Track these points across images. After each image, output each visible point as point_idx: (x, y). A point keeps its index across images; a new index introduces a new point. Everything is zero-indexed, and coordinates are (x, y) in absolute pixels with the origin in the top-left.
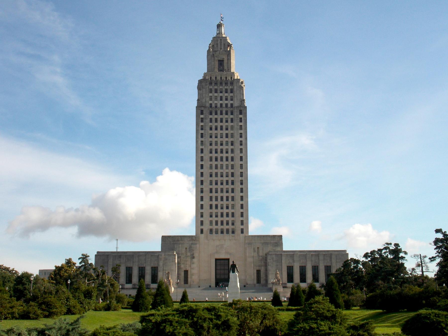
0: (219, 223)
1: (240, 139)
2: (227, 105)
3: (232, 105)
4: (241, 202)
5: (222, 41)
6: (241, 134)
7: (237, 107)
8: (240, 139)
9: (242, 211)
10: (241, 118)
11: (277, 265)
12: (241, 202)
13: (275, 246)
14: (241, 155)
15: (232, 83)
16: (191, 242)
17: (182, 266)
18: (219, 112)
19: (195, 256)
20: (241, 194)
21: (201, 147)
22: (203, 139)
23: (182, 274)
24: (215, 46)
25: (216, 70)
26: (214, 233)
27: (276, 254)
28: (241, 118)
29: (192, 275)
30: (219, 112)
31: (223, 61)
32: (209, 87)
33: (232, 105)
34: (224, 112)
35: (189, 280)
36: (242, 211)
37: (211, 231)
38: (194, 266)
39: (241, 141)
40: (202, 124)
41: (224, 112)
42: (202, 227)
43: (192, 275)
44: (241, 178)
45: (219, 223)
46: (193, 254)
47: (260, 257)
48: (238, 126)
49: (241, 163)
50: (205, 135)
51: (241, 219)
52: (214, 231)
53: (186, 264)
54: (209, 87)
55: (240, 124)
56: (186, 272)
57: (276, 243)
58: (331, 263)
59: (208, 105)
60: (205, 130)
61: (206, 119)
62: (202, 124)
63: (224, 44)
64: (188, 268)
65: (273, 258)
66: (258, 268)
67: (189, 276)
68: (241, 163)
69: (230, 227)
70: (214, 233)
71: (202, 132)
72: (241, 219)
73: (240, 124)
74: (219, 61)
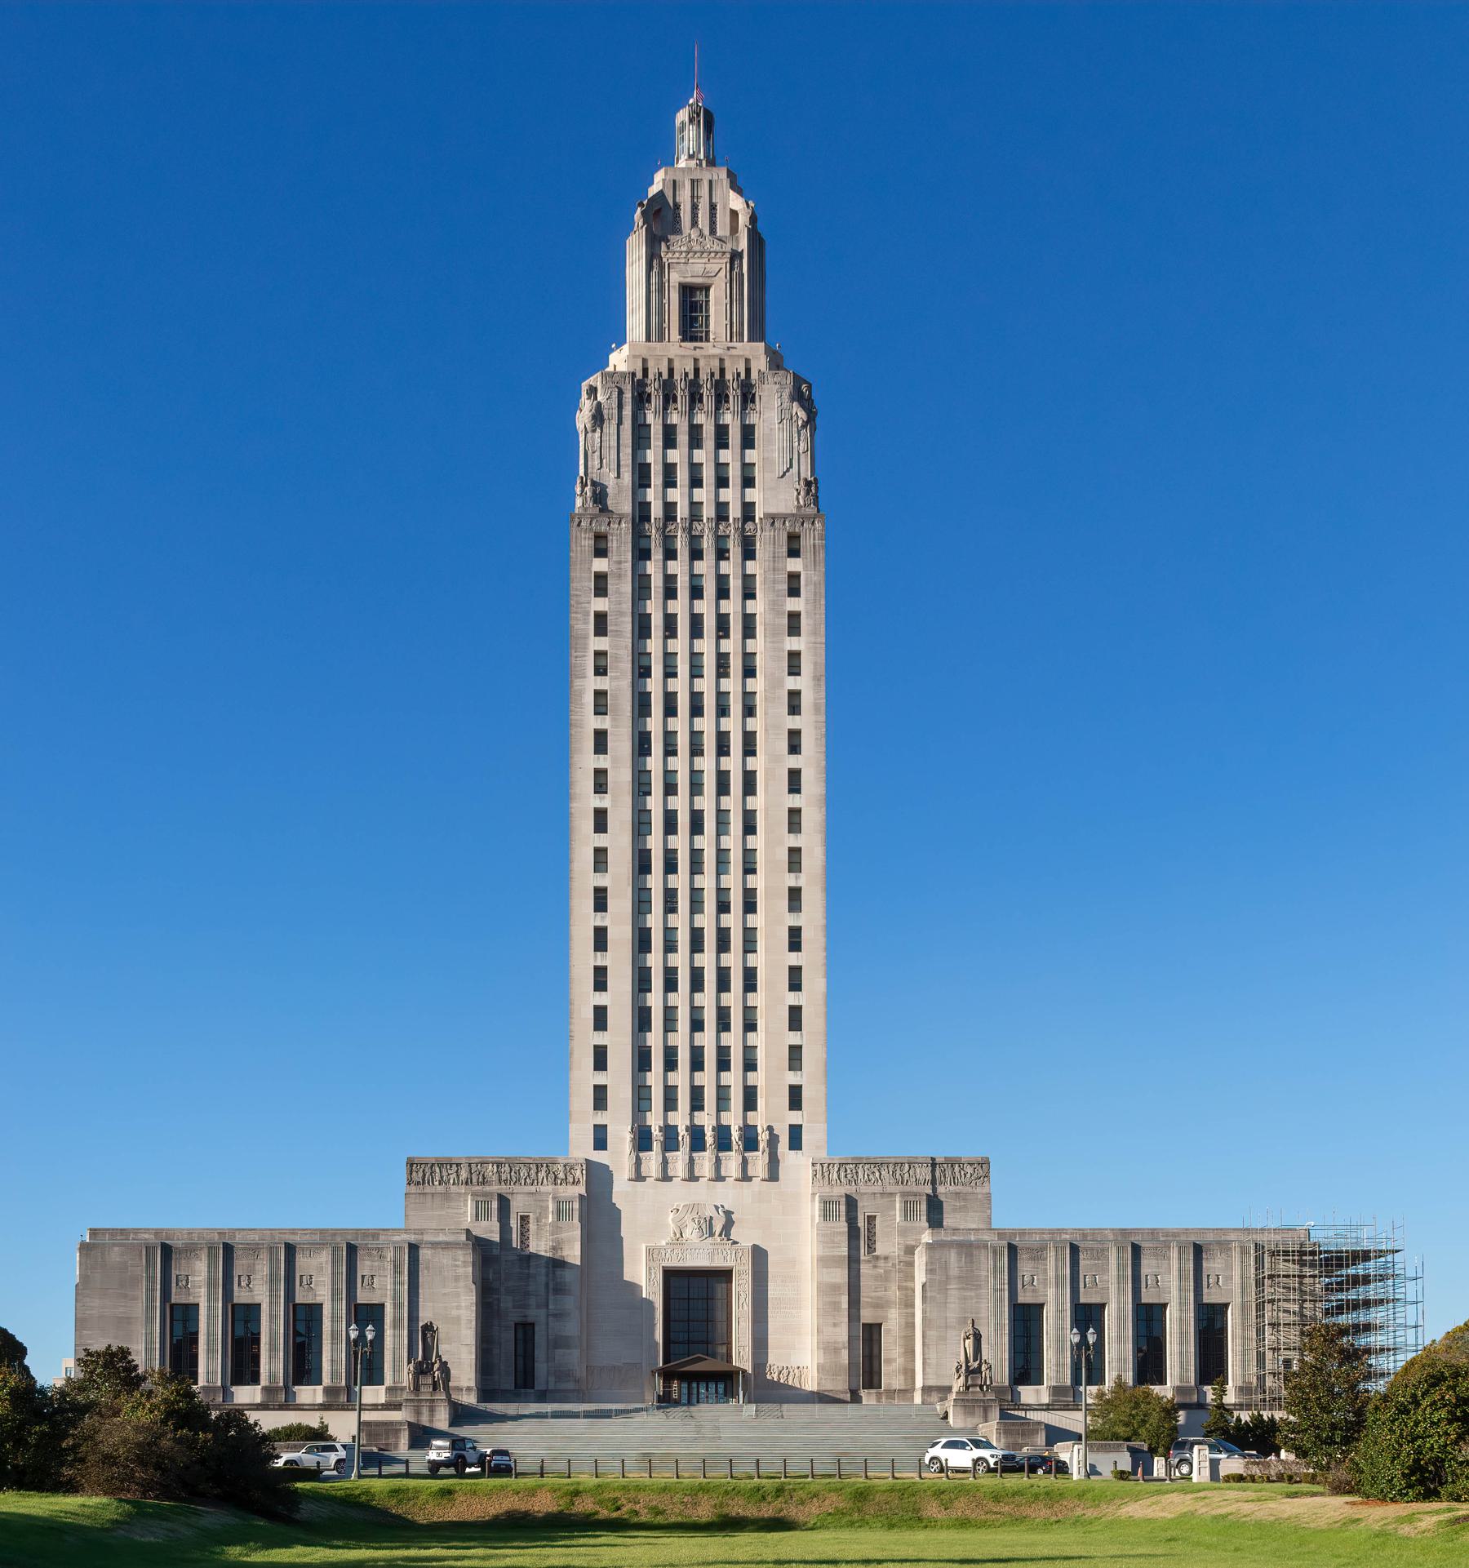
1: (792, 683)
3: (748, 509)
4: (793, 999)
5: (704, 191)
7: (773, 518)
8: (792, 683)
9: (794, 1038)
10: (794, 577)
11: (965, 1298)
12: (793, 999)
14: (794, 762)
15: (748, 397)
17: (507, 1302)
20: (794, 959)
21: (594, 723)
23: (507, 1338)
25: (675, 334)
28: (794, 577)
29: (559, 1342)
35: (541, 1368)
36: (794, 1038)
38: (569, 1303)
39: (794, 695)
40: (601, 604)
43: (559, 1342)
44: (791, 880)
48: (779, 613)
51: (793, 1078)
53: (527, 1294)
55: (793, 604)
56: (525, 1330)
62: (601, 604)
64: (535, 1314)
65: (945, 1267)
67: (540, 1354)
68: (795, 801)
70: (656, 1146)
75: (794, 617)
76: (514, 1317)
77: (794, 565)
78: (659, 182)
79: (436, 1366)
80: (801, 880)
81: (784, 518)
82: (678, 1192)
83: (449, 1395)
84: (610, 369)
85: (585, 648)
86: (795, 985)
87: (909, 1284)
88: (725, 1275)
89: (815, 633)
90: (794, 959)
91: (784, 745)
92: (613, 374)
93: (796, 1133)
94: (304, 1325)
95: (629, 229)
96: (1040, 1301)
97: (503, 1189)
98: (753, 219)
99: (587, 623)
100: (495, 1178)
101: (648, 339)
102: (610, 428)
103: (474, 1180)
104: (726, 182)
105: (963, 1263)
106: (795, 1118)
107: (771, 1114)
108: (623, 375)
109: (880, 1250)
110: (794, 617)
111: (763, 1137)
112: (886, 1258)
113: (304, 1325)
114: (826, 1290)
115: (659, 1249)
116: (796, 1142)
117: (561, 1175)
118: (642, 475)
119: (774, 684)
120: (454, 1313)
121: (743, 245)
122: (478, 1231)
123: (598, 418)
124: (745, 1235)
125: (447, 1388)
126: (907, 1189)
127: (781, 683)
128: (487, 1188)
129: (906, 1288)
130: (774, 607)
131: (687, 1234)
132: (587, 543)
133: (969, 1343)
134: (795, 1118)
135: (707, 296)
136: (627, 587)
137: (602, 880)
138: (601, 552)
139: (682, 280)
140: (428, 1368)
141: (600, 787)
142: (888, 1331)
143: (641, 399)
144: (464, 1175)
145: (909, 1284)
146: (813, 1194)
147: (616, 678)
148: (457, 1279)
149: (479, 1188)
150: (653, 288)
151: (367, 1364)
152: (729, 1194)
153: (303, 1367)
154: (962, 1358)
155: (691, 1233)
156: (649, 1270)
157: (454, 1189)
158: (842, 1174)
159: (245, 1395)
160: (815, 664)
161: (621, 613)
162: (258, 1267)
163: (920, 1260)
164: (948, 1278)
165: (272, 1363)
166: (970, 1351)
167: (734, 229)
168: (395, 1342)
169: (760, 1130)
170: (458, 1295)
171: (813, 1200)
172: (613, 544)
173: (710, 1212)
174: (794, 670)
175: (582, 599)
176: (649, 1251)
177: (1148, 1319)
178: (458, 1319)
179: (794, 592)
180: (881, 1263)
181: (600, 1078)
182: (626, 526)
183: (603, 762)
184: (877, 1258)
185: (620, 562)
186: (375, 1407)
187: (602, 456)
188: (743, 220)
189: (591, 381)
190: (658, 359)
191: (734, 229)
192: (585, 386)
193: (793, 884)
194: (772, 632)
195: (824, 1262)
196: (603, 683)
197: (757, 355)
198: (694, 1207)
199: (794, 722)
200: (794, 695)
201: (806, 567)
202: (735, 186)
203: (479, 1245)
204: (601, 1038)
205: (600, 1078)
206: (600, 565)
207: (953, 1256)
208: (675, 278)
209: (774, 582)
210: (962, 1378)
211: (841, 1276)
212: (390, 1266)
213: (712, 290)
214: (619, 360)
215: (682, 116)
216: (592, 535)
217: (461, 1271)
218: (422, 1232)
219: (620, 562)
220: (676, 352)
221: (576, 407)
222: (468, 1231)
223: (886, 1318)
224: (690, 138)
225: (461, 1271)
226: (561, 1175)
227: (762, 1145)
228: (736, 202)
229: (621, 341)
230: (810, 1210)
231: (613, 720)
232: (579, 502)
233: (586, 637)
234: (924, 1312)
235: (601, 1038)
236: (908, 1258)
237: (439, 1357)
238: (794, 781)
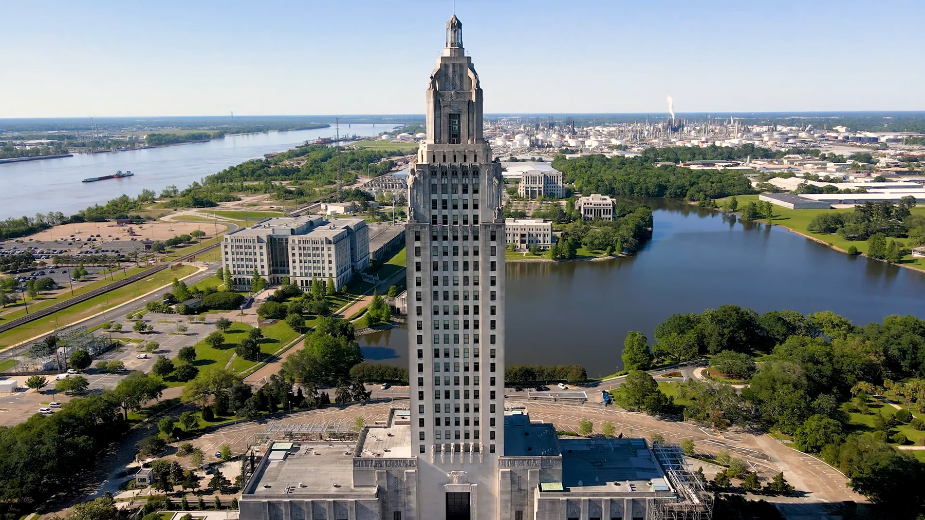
7: (486, 226)
9: (492, 416)
17: (390, 505)
21: (417, 304)
32: (430, 181)
40: (418, 259)
54: (430, 181)
55: (492, 259)
60: (425, 271)
61: (425, 248)
62: (418, 259)
66: (518, 509)
75: (493, 264)
76: (394, 509)
77: (493, 243)
80: (495, 361)
110: (493, 264)
116: (493, 451)
119: (485, 289)
127: (488, 289)
130: (485, 259)
132: (413, 236)
138: (418, 239)
172: (422, 236)
174: (493, 283)
179: (493, 254)
181: (422, 430)
183: (420, 318)
196: (419, 289)
205: (422, 430)
238: (493, 339)
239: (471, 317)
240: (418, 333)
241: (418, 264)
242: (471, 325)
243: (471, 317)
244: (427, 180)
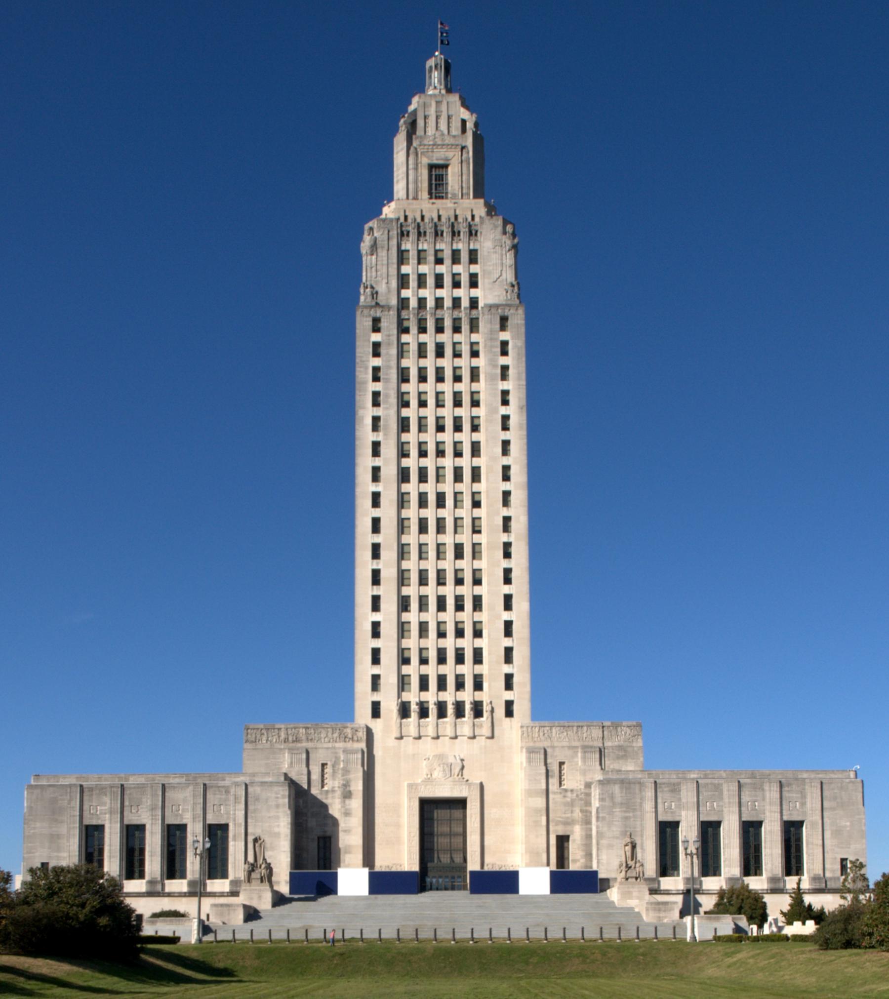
0: (433, 684)
1: (503, 410)
2: (456, 302)
3: (474, 303)
5: (444, 107)
6: (505, 393)
7: (490, 307)
8: (503, 410)
9: (508, 642)
11: (627, 818)
12: (506, 616)
13: (619, 758)
14: (505, 461)
15: (472, 233)
16: (340, 745)
18: (430, 325)
19: (352, 788)
20: (507, 590)
21: (372, 437)
22: (378, 412)
24: (420, 123)
25: (425, 195)
26: (414, 715)
27: (622, 782)
30: (430, 325)
31: (446, 166)
33: (474, 303)
34: (448, 324)
37: (404, 711)
39: (505, 418)
40: (377, 362)
41: (448, 324)
42: (376, 697)
45: (433, 684)
46: (346, 785)
47: (569, 794)
48: (495, 366)
49: (506, 486)
50: (387, 396)
51: (507, 669)
52: (414, 707)
54: (399, 246)
55: (504, 361)
57: (620, 748)
58: (804, 813)
59: (394, 302)
60: (387, 381)
62: (377, 362)
63: (449, 117)
65: (612, 797)
68: (506, 486)
69: (467, 696)
71: (378, 387)
72: (507, 669)
73: (504, 361)
74: (431, 167)
78: (415, 103)
79: (263, 866)
80: (512, 538)
81: (497, 306)
82: (427, 746)
83: (271, 886)
84: (383, 216)
85: (366, 390)
86: (508, 606)
87: (588, 808)
88: (460, 803)
89: (519, 379)
90: (507, 590)
91: (499, 450)
92: (384, 220)
93: (509, 705)
94: (174, 835)
95: (395, 131)
96: (677, 819)
97: (309, 745)
98: (476, 125)
99: (366, 373)
100: (304, 737)
101: (408, 198)
102: (383, 253)
103: (290, 739)
104: (458, 103)
105: (624, 794)
106: (508, 695)
107: (493, 694)
108: (391, 220)
109: (567, 785)
110: (505, 369)
111: (486, 708)
112: (572, 791)
113: (174, 835)
114: (531, 812)
115: (417, 785)
116: (509, 713)
117: (350, 736)
118: (403, 282)
119: (492, 411)
120: (276, 830)
121: (469, 141)
122: (293, 776)
123: (374, 247)
124: (475, 776)
125: (270, 881)
126: (586, 743)
127: (496, 411)
128: (299, 745)
129: (586, 811)
130: (492, 363)
131: (436, 774)
132: (369, 323)
133: (628, 848)
134: (508, 695)
135: (447, 171)
136: (394, 351)
137: (377, 539)
138: (376, 329)
139: (430, 162)
140: (258, 869)
141: (376, 478)
142: (574, 841)
143: (403, 234)
144: (283, 736)
145: (588, 808)
146: (522, 748)
147: (387, 409)
148: (278, 806)
149: (294, 745)
150: (411, 166)
151: (215, 863)
152: (462, 749)
153: (173, 866)
154: (624, 859)
155: (437, 774)
156: (410, 799)
157: (278, 746)
158: (541, 734)
159: (132, 886)
160: (519, 398)
161: (389, 367)
162: (144, 800)
163: (595, 793)
164: (614, 803)
165: (153, 864)
166: (629, 854)
167: (464, 130)
168: (236, 850)
169: (485, 704)
170: (278, 817)
171: (522, 752)
172: (383, 324)
173: (451, 760)
175: (364, 359)
176: (410, 786)
177: (751, 831)
178: (277, 835)
179: (504, 353)
180: (569, 794)
181: (376, 670)
182: (393, 313)
184: (566, 790)
185: (389, 336)
186: (222, 895)
187: (377, 271)
188: (470, 125)
189: (370, 224)
190: (414, 211)
191: (464, 130)
192: (367, 227)
193: (506, 540)
194: (491, 378)
195: (530, 793)
197: (479, 208)
198: (440, 757)
199: (505, 435)
200: (505, 418)
201: (513, 338)
202: (464, 105)
203: (293, 785)
204: (376, 643)
205: (376, 670)
206: (376, 337)
207: (616, 789)
208: (425, 161)
209: (492, 347)
210: (624, 872)
211: (541, 802)
212: (232, 798)
213: (450, 169)
214: (389, 211)
215: (431, 62)
216: (371, 319)
217: (281, 801)
218: (254, 775)
219: (389, 336)
220: (428, 208)
221: (361, 239)
222: (286, 775)
223: (572, 832)
224: (436, 77)
225: (281, 801)
226: (350, 736)
227: (485, 714)
228: (465, 114)
229: (390, 199)
230: (520, 758)
231: (385, 435)
232: (362, 298)
233: (365, 383)
234: (597, 827)
235: (376, 643)
236: (587, 791)
237: (264, 859)
239: (466, 462)
240: (373, 488)
241: (376, 370)
242: (467, 475)
243: (466, 462)
244: (394, 242)
